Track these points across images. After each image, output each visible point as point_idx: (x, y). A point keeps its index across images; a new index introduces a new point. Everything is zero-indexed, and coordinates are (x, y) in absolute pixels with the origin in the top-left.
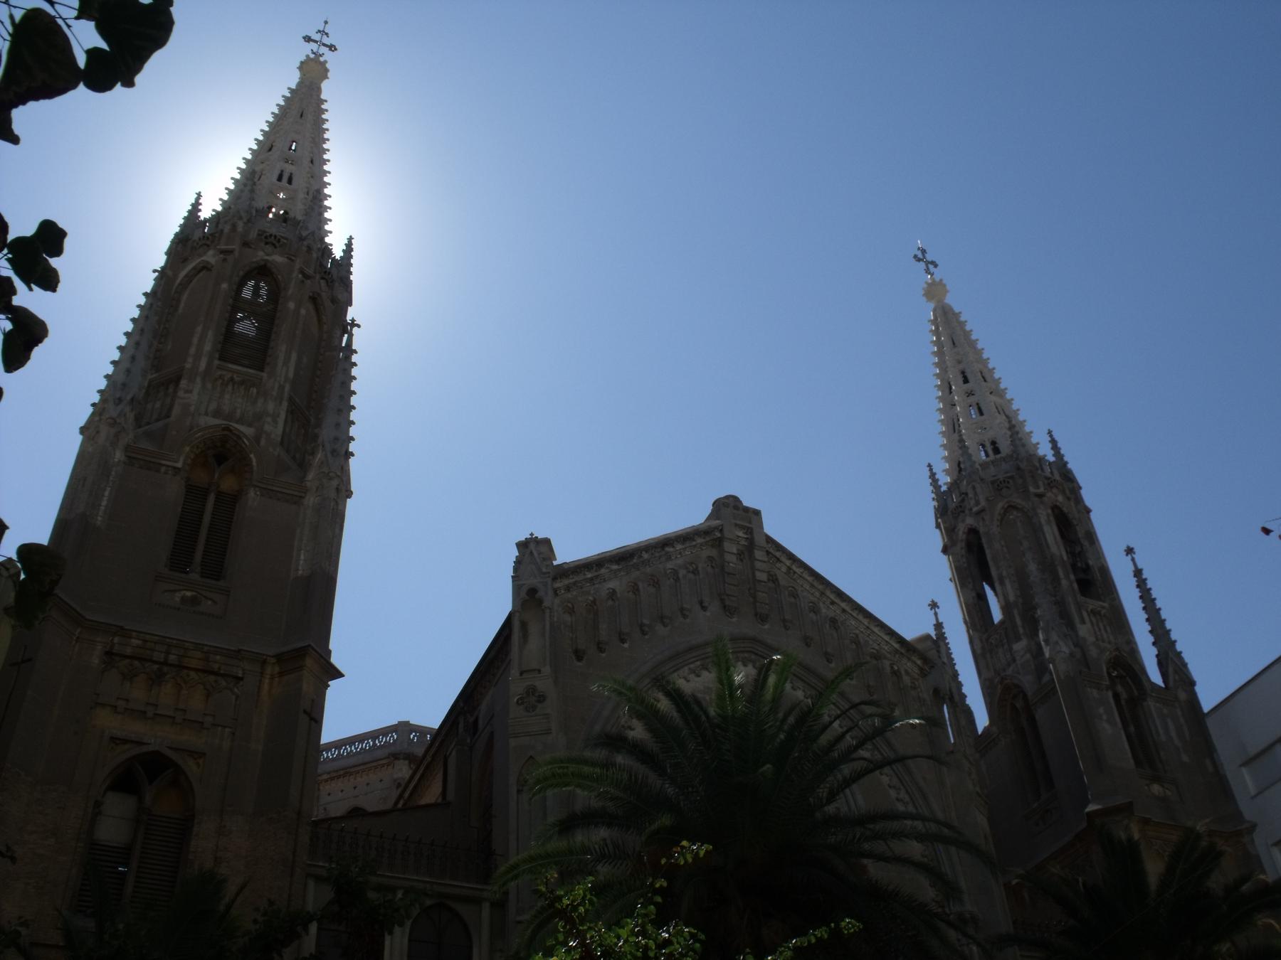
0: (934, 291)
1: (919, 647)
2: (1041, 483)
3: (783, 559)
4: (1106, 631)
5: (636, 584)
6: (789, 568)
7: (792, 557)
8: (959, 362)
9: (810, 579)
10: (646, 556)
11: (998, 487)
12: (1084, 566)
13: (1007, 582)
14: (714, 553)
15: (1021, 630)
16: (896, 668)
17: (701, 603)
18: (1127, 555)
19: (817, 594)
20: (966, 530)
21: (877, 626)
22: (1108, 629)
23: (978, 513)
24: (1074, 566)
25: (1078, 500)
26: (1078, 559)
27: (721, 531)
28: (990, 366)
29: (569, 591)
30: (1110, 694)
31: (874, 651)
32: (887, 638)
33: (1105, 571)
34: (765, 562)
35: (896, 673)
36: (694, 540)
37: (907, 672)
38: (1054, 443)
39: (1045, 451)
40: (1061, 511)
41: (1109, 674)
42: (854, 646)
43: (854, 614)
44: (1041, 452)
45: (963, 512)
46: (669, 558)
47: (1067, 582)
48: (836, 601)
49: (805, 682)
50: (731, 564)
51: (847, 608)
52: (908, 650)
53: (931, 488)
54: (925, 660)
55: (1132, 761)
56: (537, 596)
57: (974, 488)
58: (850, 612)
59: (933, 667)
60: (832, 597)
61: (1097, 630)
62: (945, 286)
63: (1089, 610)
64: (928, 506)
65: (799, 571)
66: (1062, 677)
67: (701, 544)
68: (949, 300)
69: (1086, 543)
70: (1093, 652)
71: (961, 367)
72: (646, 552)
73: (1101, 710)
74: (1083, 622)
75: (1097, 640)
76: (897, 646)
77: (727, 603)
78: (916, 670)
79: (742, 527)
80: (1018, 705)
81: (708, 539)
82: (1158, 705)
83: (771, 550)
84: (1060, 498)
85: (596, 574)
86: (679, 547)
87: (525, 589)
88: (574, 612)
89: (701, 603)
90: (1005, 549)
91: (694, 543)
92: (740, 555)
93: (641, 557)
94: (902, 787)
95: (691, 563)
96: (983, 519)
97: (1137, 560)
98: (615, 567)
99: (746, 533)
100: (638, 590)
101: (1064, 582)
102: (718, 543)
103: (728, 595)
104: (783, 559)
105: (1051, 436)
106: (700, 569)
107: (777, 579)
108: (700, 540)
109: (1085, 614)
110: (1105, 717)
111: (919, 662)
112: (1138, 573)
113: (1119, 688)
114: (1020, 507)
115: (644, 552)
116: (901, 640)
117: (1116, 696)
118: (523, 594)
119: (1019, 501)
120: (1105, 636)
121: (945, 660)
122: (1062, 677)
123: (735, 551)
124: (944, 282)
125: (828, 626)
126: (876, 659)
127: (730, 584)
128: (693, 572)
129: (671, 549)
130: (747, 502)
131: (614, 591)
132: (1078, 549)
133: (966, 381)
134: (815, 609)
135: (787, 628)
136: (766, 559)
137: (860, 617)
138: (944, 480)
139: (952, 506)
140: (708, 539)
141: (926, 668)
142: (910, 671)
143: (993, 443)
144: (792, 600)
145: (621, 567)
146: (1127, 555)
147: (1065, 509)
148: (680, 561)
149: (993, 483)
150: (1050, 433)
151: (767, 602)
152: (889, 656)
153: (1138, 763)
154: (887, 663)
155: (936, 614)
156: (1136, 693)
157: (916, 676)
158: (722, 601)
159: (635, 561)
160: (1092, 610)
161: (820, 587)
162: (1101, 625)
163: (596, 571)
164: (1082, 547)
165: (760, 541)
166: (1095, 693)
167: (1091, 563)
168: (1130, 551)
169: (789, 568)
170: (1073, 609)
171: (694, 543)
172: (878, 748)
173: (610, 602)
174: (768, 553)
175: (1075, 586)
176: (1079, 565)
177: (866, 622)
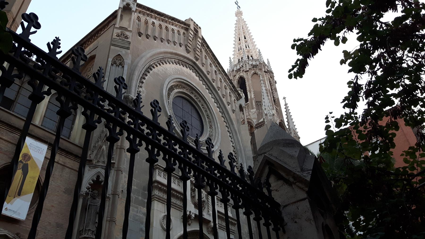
0: (239, 14)
15: (254, 106)
23: (246, 72)
25: (273, 79)
29: (140, 13)
45: (240, 71)
46: (173, 25)
53: (229, 64)
57: (246, 64)
59: (241, 98)
87: (125, 3)
88: (140, 21)
100: (162, 28)
105: (268, 60)
112: (286, 105)
139: (235, 69)
149: (251, 65)
158: (186, 47)
173: (152, 26)
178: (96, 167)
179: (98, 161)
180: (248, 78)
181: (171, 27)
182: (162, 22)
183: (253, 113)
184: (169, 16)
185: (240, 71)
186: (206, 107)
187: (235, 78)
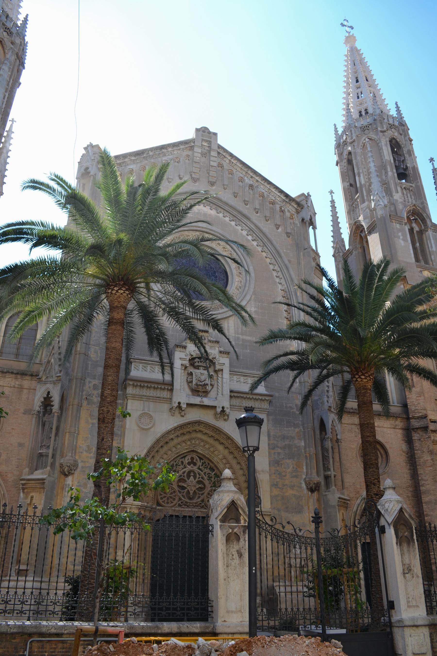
1: (298, 200)
2: (384, 126)
3: (227, 156)
4: (411, 198)
5: (145, 167)
6: (230, 161)
7: (231, 155)
8: (356, 73)
9: (240, 166)
10: (151, 153)
11: (364, 129)
12: (405, 167)
13: (361, 175)
14: (190, 153)
16: (283, 209)
17: (179, 176)
18: (430, 162)
19: (244, 173)
20: (347, 153)
21: (275, 188)
22: (413, 197)
23: (351, 143)
24: (397, 168)
26: (402, 164)
27: (194, 142)
28: (372, 73)
30: (407, 228)
31: (272, 201)
32: (279, 194)
33: (415, 169)
34: (216, 157)
35: (282, 211)
36: (179, 147)
37: (288, 210)
38: (398, 107)
39: (393, 112)
40: (396, 141)
41: (408, 218)
42: (261, 198)
43: (263, 183)
44: (391, 113)
46: (165, 155)
47: (392, 173)
48: (253, 176)
49: (230, 213)
50: (197, 158)
51: (259, 180)
52: (290, 200)
54: (298, 204)
55: (413, 260)
56: (88, 171)
58: (260, 181)
59: (302, 208)
60: (251, 174)
61: (406, 197)
62: (355, 37)
63: (403, 187)
64: (333, 143)
65: (235, 162)
66: (379, 217)
67: (183, 149)
68: (358, 45)
69: (406, 156)
70: (400, 207)
71: (356, 75)
72: (151, 151)
73: (400, 234)
74: (397, 192)
75: (405, 201)
76: (284, 198)
77: (193, 176)
78: (294, 210)
79: (206, 141)
80: (362, 235)
81: (187, 146)
82: (434, 233)
83: (221, 152)
84: (396, 134)
85: (123, 161)
86: (170, 149)
89: (179, 176)
90: (363, 160)
91: (179, 148)
92: (203, 154)
93: (148, 153)
94: (276, 264)
95: (177, 158)
96: (354, 146)
97: (434, 165)
98: (133, 158)
99: (208, 144)
100: (145, 169)
101: (390, 174)
102: (192, 148)
103: (194, 173)
104: (227, 156)
106: (181, 160)
107: (223, 166)
108: (182, 147)
109: (399, 189)
110: (401, 237)
111: (295, 206)
113: (414, 225)
114: (373, 138)
115: (150, 152)
116: (287, 196)
117: (411, 230)
118: (82, 170)
119: (373, 136)
120: (410, 200)
121: (309, 205)
122: (379, 217)
123: (200, 152)
124: (355, 35)
125: (247, 188)
126: (272, 204)
127: (195, 167)
128: (178, 162)
129: (166, 151)
130: (212, 130)
131: (132, 170)
132: (402, 159)
133: (357, 81)
134: (241, 180)
135: (225, 189)
136: (217, 156)
137: (266, 184)
138: (340, 131)
140: (187, 146)
141: (299, 209)
142: (291, 210)
143: (366, 110)
144: (231, 176)
145: (136, 158)
146: (430, 162)
147: (398, 140)
148: (171, 157)
149: (361, 128)
150: (396, 104)
151: (215, 176)
152: (280, 203)
153: (417, 260)
154: (278, 207)
155: (332, 196)
156: (423, 228)
157: (294, 213)
158: (191, 175)
159: (145, 155)
160: (404, 188)
161: (246, 170)
162: (409, 195)
163: (123, 160)
164: (405, 158)
165: (214, 147)
166: (398, 226)
167: (408, 165)
168: (432, 160)
169: (230, 161)
170: (392, 186)
171: (179, 148)
172: (266, 246)
174: (219, 153)
175: (396, 175)
176: (402, 166)
177: (268, 186)
178: (45, 383)
179: (47, 377)
180: (355, 153)
181: (162, 160)
182: (146, 162)
183: (364, 209)
184: (153, 148)
185: (346, 144)
186: (230, 249)
187: (342, 158)
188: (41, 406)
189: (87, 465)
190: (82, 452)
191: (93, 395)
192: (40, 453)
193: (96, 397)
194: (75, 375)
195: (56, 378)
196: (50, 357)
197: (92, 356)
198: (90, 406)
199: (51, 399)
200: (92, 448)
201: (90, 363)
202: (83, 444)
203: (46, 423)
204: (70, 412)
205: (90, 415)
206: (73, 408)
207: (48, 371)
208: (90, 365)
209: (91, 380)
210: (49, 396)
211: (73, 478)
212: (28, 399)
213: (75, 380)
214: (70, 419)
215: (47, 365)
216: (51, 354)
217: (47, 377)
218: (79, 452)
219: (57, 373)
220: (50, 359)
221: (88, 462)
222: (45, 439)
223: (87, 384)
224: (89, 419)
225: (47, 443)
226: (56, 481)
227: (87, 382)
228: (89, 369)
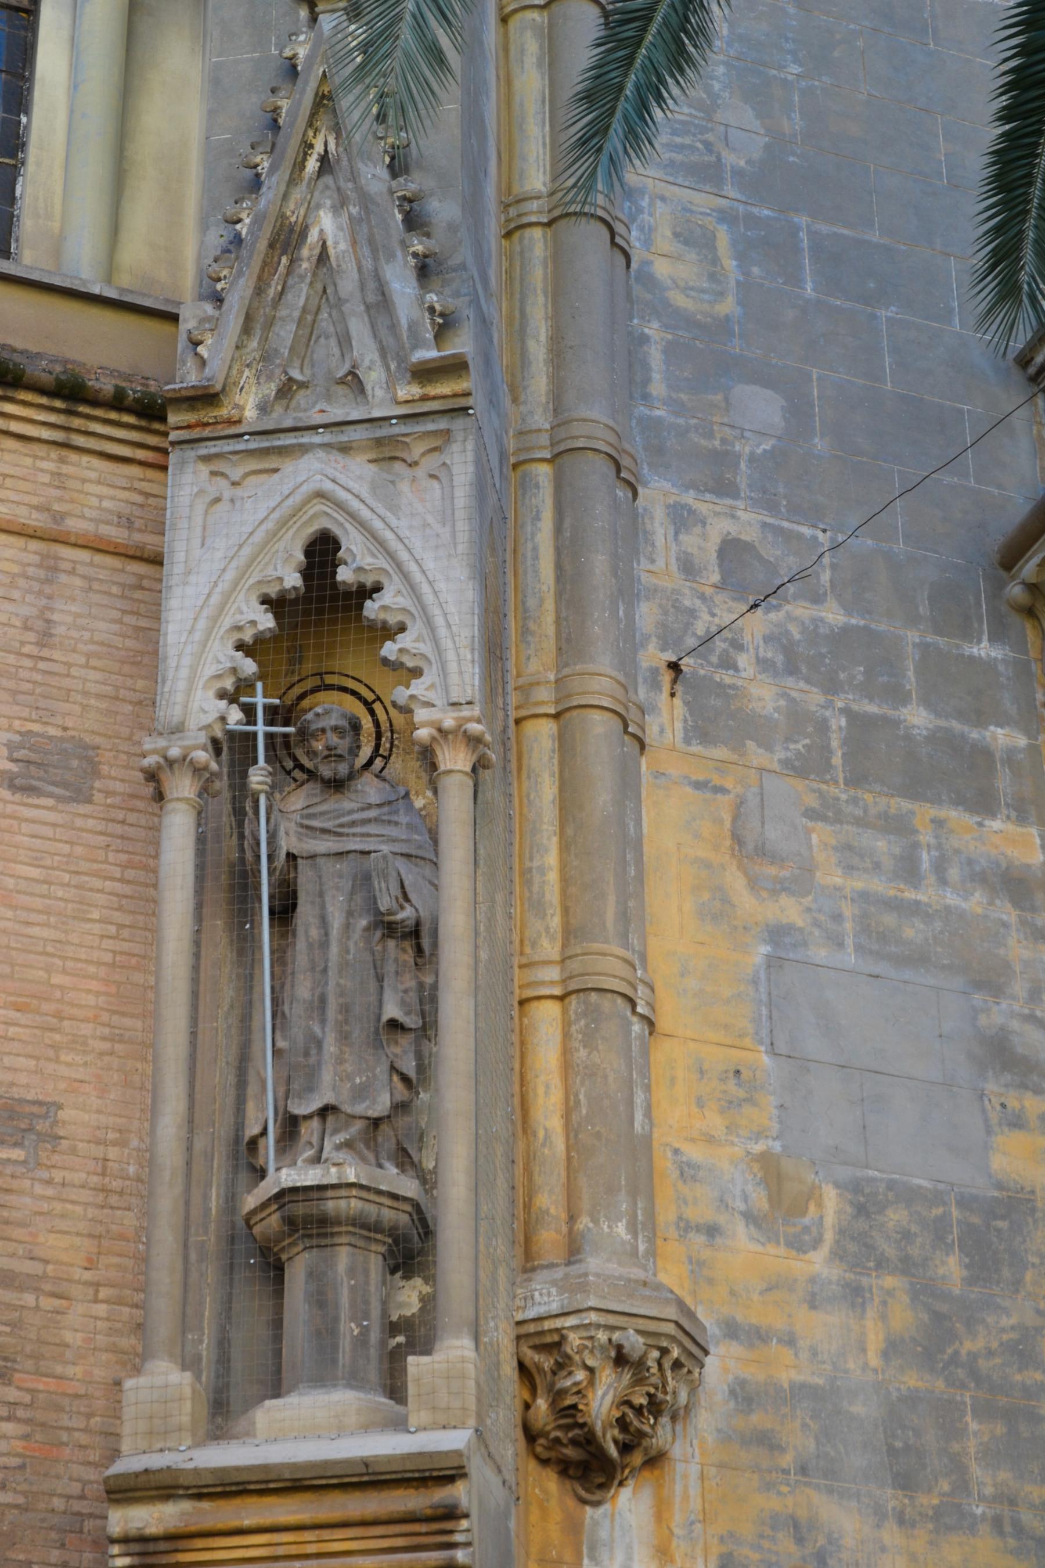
179: (287, 390)
188: (244, 686)
189: (786, 1377)
190: (712, 1231)
191: (738, 646)
192: (285, 1195)
193: (764, 664)
194: (541, 420)
195: (408, 390)
196: (298, 193)
197: (662, 269)
198: (721, 753)
199: (371, 609)
200: (813, 1194)
201: (653, 330)
202: (710, 1139)
203: (305, 879)
204: (548, 790)
205: (737, 839)
206: (565, 746)
207: (285, 333)
208: (655, 356)
209: (689, 498)
210: (344, 575)
211: (661, 1512)
212: (45, 638)
213: (543, 472)
214: (552, 859)
215: (268, 266)
216: (300, 165)
217: (287, 390)
218: (685, 1227)
219: (417, 343)
220: (294, 213)
221: (790, 1341)
222: (330, 1047)
223: (659, 528)
224: (735, 881)
225: (360, 1093)
226: (512, 1524)
227: (659, 513)
228: (658, 388)
